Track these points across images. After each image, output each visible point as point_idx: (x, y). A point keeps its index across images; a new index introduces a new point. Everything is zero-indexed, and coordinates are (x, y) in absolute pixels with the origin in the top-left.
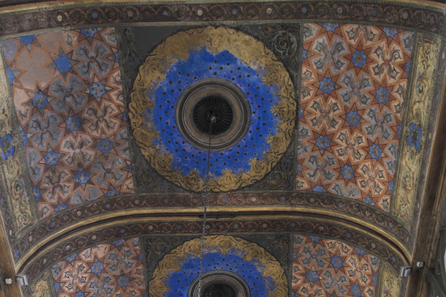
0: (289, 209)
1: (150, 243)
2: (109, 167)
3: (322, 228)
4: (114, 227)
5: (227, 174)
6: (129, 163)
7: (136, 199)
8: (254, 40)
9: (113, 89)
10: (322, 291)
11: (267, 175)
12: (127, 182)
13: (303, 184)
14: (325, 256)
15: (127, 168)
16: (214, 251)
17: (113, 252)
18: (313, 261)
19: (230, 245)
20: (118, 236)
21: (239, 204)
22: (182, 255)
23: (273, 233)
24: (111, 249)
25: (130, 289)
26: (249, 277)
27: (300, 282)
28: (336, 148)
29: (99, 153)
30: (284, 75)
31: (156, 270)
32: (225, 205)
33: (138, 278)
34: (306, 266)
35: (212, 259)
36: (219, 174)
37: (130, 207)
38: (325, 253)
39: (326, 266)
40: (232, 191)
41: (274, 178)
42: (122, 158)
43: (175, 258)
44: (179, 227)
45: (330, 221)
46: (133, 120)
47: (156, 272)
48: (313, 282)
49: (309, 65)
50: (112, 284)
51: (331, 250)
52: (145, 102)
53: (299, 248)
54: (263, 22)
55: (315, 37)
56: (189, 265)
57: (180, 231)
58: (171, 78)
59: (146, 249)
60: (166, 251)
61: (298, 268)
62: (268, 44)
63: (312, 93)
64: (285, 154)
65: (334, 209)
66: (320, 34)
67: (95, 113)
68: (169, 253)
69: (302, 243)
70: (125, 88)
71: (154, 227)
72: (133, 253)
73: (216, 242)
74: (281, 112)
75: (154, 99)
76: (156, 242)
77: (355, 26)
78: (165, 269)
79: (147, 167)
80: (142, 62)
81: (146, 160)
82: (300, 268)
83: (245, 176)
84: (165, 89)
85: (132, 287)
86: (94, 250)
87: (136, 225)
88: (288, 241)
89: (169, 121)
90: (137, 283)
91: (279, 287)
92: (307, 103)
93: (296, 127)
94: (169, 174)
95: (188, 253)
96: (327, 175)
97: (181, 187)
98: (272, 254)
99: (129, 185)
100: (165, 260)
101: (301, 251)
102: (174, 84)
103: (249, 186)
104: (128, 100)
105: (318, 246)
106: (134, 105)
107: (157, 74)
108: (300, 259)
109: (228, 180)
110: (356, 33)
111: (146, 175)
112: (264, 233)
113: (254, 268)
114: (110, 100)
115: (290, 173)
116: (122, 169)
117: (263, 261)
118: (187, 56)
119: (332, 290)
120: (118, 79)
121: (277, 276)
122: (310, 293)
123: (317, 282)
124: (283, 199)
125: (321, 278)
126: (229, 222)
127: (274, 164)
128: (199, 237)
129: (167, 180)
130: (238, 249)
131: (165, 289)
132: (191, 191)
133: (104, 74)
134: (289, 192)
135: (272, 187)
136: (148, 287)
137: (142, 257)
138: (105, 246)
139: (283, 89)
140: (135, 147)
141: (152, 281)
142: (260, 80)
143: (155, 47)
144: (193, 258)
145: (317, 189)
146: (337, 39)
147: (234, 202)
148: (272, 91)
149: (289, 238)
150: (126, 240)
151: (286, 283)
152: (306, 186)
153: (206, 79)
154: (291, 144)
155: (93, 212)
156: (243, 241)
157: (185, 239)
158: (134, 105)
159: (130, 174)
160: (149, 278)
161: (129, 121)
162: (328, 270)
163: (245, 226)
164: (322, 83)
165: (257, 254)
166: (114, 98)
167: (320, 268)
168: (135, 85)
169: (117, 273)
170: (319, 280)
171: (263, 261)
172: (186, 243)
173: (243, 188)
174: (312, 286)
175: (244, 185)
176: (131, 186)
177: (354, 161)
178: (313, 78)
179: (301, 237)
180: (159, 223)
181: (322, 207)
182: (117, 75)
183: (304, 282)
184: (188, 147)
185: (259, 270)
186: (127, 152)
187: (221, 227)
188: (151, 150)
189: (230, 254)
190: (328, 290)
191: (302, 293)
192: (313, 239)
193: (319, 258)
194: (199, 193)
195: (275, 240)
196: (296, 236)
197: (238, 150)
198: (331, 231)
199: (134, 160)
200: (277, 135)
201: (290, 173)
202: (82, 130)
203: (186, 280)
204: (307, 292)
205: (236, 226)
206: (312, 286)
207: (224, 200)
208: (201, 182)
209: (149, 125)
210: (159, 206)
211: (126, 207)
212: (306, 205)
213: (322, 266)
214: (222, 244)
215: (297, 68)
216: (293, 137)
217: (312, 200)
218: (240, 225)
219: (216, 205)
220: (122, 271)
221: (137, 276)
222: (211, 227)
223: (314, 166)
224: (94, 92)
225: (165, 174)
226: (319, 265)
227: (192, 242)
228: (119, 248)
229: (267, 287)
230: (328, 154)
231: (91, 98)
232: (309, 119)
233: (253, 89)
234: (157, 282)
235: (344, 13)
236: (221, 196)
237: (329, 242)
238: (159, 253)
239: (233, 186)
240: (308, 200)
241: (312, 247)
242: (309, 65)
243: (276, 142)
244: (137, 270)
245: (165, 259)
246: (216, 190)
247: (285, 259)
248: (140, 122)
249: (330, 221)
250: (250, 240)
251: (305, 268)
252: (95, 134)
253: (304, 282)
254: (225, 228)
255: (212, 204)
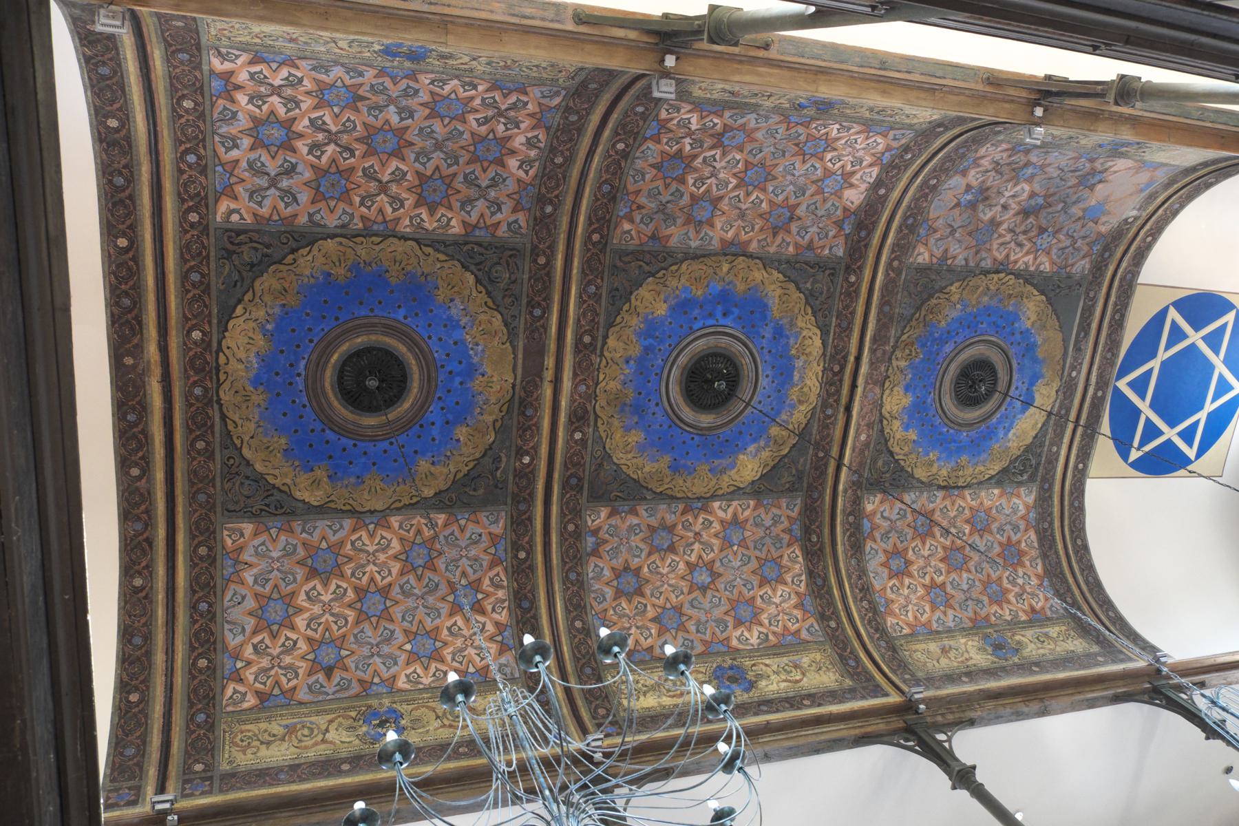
0: (841, 487)
1: (828, 272)
2: (957, 235)
3: (814, 538)
4: (875, 224)
5: (904, 400)
6: (949, 262)
7: (901, 262)
8: (1034, 433)
9: (1035, 259)
10: (712, 555)
11: (891, 454)
12: (927, 255)
13: (871, 504)
14: (773, 550)
15: (944, 257)
16: (796, 376)
17: (839, 212)
18: (760, 532)
19: (800, 402)
20: (860, 226)
21: (861, 417)
22: (800, 324)
23: (808, 466)
24: (845, 209)
25: (759, 224)
26: (741, 433)
27: (721, 514)
28: (918, 542)
29: (981, 225)
30: (995, 468)
31: (780, 276)
32: (864, 396)
33: (773, 243)
34: (751, 521)
35: (784, 373)
36: (907, 388)
37: (893, 251)
38: (777, 549)
39: (758, 553)
40: (881, 406)
41: (885, 463)
42: (959, 253)
43: (796, 311)
44: (845, 324)
45: (828, 550)
46: (995, 277)
47: (775, 273)
48: (724, 537)
49: (1001, 496)
50: (787, 199)
51: (786, 557)
52: (1010, 296)
53: (780, 508)
54: (1047, 443)
55: (1024, 499)
56: (779, 333)
57: (839, 325)
58: (1025, 333)
59: (819, 265)
60: (810, 297)
61: (746, 509)
62: (1028, 449)
63: (973, 503)
64: (912, 476)
65: (845, 551)
66: (1027, 506)
67: (1025, 232)
68: (807, 302)
69: (788, 510)
70: (1032, 275)
71: (853, 284)
72: (821, 243)
73: (810, 379)
74: (959, 467)
75: (1011, 308)
76: (826, 281)
77: (1036, 545)
78: (779, 291)
79: (937, 287)
80: (1048, 299)
81: (946, 287)
82: (747, 513)
83: (896, 424)
84: (1016, 325)
85: (761, 230)
86: (863, 187)
87: (863, 256)
88: (792, 489)
89: (984, 325)
90: (765, 239)
91: (713, 483)
92: (964, 498)
93: (941, 488)
94: (921, 319)
95: (800, 333)
96: (885, 536)
97: (903, 334)
98: (774, 467)
99: (922, 256)
100: (796, 295)
101: (775, 511)
102: (1018, 337)
103: (882, 431)
104: (1017, 275)
105: (786, 537)
106: (1011, 283)
107: (1033, 317)
108: (762, 510)
109: (896, 401)
110: (1031, 547)
111: (929, 284)
112: (811, 452)
113: (754, 440)
114: (1027, 253)
115: (887, 485)
116: (946, 251)
117: (765, 454)
118: (1040, 356)
119: (721, 570)
120: (1042, 268)
121: (736, 477)
122: (704, 534)
123: (727, 543)
124: (855, 478)
125: (735, 548)
126: (837, 401)
127: (902, 463)
128: (824, 354)
129: (914, 314)
130: (792, 414)
131: (741, 287)
132: (895, 347)
133: (1054, 251)
134: (861, 486)
135: (874, 461)
136: (751, 256)
137: (809, 256)
138: (857, 203)
139: (982, 469)
140: (967, 274)
141: (761, 266)
142: (997, 441)
143: (1058, 319)
144: (792, 341)
145: (866, 525)
146: (1022, 526)
147: (865, 410)
148: (984, 456)
149: (796, 490)
150: (847, 236)
151: (720, 492)
152: (869, 508)
153: (1015, 377)
154: (922, 483)
155: (918, 199)
156: (804, 421)
157: (824, 332)
158: (1011, 283)
159: (935, 260)
160: (767, 262)
161: (997, 272)
162: (753, 559)
163: (825, 427)
164: (982, 514)
165: (778, 443)
166: (1026, 259)
167: (751, 545)
168: (1029, 288)
169: (801, 211)
170: (731, 546)
171: (765, 454)
172: (819, 333)
173: (881, 422)
174: (716, 535)
175: (885, 422)
176: (920, 260)
177: (914, 569)
178: (987, 503)
179: (796, 509)
180: (857, 292)
181: (844, 534)
182: (1046, 267)
183: (722, 522)
184: (948, 348)
185: (752, 448)
186: (963, 263)
187: (833, 389)
188: (957, 296)
189: (788, 402)
190: (718, 564)
191: (701, 520)
192: (794, 527)
193: (768, 541)
194: (890, 359)
195: (797, 470)
196: (799, 501)
197: (931, 414)
198: (813, 554)
199: (950, 270)
200: (936, 465)
201: (887, 485)
202: (1018, 213)
203: (753, 326)
204: (703, 529)
205: (829, 412)
206: (716, 535)
207: (870, 395)
208: (903, 364)
209: (986, 299)
210: (883, 296)
211: (896, 246)
212: (844, 511)
213: (755, 548)
214: (805, 390)
215: (999, 483)
216: (929, 485)
217: (851, 519)
218: (829, 417)
219: (867, 383)
220: (800, 219)
221: (779, 239)
222: (835, 374)
223: (894, 517)
224: (1045, 236)
225: (923, 313)
226: (755, 542)
227: (818, 342)
228: (839, 224)
229: (717, 462)
230: (910, 532)
231: (1042, 230)
232: (947, 502)
233: (990, 434)
234: (758, 275)
235: (1045, 530)
236: (878, 390)
237: (798, 552)
238: (809, 285)
239: (887, 407)
240: (850, 514)
241: (782, 527)
242: (1001, 496)
243: (929, 465)
244: (788, 244)
245: (798, 294)
246: (887, 384)
247: (761, 489)
248: (992, 287)
249: (828, 550)
250: (803, 433)
251: (747, 521)
252: (1005, 226)
253: (722, 522)
254: (829, 395)
255: (869, 377)
